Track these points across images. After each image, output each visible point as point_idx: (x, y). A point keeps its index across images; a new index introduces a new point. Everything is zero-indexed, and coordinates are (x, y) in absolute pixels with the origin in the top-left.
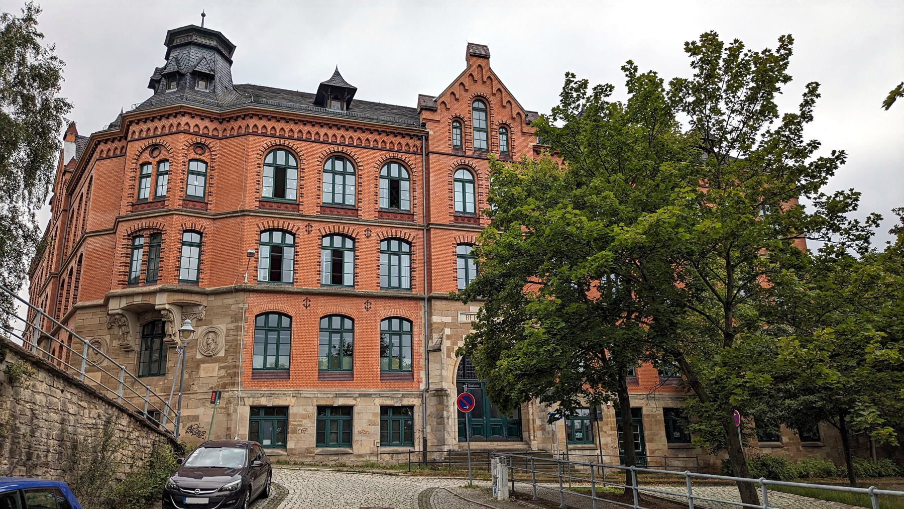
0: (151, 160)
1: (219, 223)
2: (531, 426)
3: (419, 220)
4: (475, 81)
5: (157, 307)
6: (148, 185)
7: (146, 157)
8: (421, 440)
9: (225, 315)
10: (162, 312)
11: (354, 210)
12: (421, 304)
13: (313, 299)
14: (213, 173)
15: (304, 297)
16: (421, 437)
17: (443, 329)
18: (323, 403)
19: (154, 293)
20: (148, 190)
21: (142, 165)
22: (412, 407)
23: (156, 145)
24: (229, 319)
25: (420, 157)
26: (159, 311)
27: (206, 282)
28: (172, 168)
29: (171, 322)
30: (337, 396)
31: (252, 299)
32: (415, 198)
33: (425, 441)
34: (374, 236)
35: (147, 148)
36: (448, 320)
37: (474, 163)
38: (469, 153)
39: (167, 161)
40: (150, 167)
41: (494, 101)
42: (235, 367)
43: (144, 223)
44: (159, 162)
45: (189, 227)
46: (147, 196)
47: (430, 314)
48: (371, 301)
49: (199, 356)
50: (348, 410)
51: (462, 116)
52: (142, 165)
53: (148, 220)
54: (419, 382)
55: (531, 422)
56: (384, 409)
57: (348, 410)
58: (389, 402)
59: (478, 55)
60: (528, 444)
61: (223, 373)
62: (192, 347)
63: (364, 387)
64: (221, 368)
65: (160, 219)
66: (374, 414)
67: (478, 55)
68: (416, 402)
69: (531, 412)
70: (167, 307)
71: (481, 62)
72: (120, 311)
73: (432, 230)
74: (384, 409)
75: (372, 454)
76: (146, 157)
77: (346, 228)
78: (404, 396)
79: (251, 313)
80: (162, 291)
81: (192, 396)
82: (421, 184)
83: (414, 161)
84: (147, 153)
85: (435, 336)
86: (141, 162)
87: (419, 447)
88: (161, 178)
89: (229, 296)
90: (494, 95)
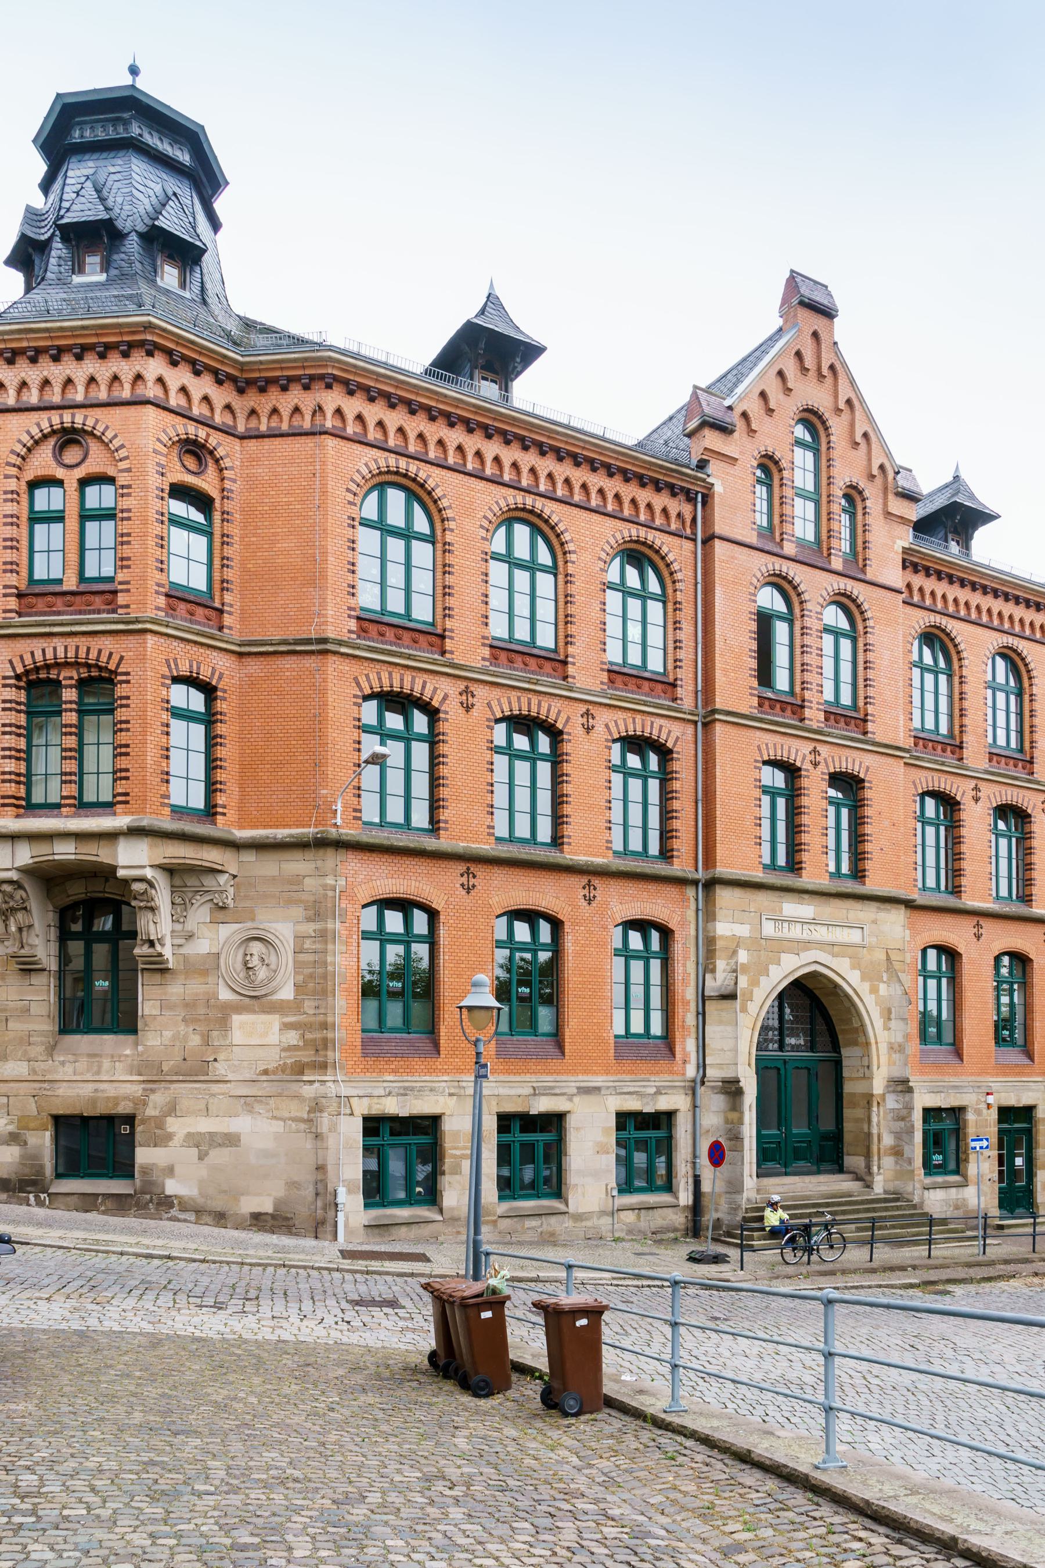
0: (60, 473)
1: (254, 667)
2: (875, 1148)
3: (686, 694)
4: (804, 370)
5: (121, 873)
6: (57, 544)
7: (44, 462)
8: (691, 1180)
9: (290, 902)
10: (137, 887)
11: (557, 662)
12: (690, 892)
13: (478, 870)
14: (228, 528)
15: (461, 867)
16: (690, 1173)
17: (735, 953)
18: (510, 1108)
19: (111, 836)
20: (57, 558)
21: (34, 485)
22: (669, 1116)
23: (73, 430)
24: (298, 912)
25: (688, 545)
26: (126, 882)
27: (232, 814)
28: (124, 503)
29: (152, 909)
30: (535, 1093)
31: (353, 865)
32: (677, 644)
33: (697, 1181)
34: (600, 728)
35: (45, 437)
36: (743, 930)
37: (798, 573)
38: (789, 549)
39: (111, 480)
40: (56, 492)
41: (837, 426)
42: (324, 1026)
43: (59, 648)
44: (84, 482)
45: (184, 670)
46: (56, 573)
48: (596, 882)
49: (225, 995)
50: (555, 1121)
51: (778, 455)
52: (34, 485)
53: (72, 642)
54: (685, 1062)
56: (623, 1119)
57: (555, 1121)
58: (633, 1105)
59: (809, 304)
60: (864, 1178)
61: (293, 1038)
62: (205, 973)
63: (586, 1072)
64: (286, 1027)
65: (107, 644)
66: (606, 1130)
67: (809, 304)
68: (675, 1101)
69: (875, 1119)
70: (149, 873)
71: (817, 322)
72: (14, 875)
73: (718, 727)
74: (623, 1119)
75: (603, 1213)
76: (44, 462)
77: (545, 706)
78: (658, 1092)
79: (352, 898)
80: (136, 832)
81: (215, 1088)
82: (691, 612)
83: (678, 552)
84: (46, 451)
85: (721, 965)
86: (29, 475)
87: (685, 1198)
88: (91, 527)
89: (298, 854)
90: (838, 411)
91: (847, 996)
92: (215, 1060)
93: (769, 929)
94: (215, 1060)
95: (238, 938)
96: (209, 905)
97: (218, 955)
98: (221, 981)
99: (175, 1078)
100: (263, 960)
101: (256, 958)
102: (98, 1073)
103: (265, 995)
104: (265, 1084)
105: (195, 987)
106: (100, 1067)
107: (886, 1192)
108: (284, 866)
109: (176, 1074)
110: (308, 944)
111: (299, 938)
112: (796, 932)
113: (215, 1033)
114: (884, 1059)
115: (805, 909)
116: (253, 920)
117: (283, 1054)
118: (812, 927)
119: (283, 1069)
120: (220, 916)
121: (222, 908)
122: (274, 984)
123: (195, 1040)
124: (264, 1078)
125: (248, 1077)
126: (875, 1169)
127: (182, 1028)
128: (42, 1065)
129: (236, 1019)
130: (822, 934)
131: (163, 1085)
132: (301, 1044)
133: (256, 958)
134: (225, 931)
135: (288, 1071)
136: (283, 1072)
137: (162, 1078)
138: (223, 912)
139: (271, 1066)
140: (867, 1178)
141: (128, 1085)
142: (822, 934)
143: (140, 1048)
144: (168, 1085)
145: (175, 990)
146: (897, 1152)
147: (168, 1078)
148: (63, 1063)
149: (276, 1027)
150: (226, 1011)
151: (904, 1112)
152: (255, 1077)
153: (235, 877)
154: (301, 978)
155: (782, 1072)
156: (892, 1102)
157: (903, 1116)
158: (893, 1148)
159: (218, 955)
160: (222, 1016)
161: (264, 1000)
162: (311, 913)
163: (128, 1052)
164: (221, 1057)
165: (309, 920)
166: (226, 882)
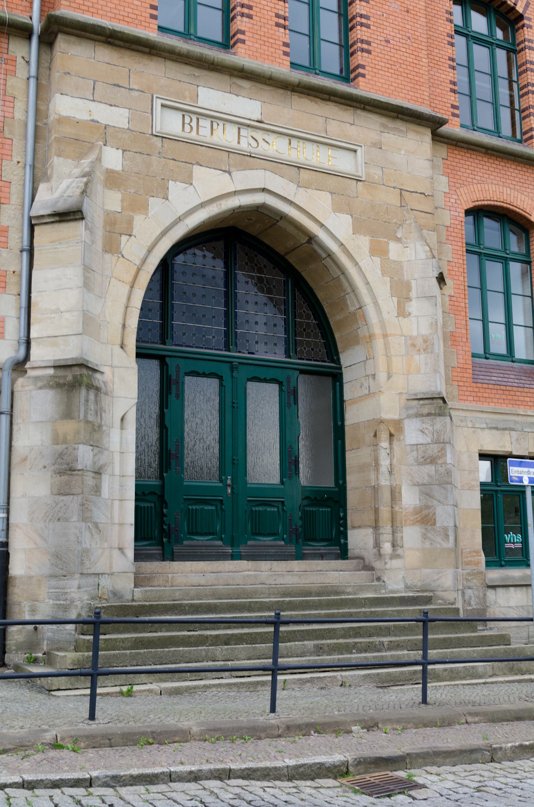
2: (385, 513)
36: (117, 117)
47: (42, 90)
55: (386, 495)
69: (384, 462)
91: (330, 255)
93: (171, 123)
107: (408, 588)
112: (226, 137)
114: (398, 364)
115: (246, 105)
118: (259, 135)
126: (387, 547)
130: (276, 147)
140: (377, 565)
142: (276, 147)
146: (425, 518)
151: (434, 450)
155: (228, 382)
156: (413, 433)
157: (431, 457)
158: (418, 511)
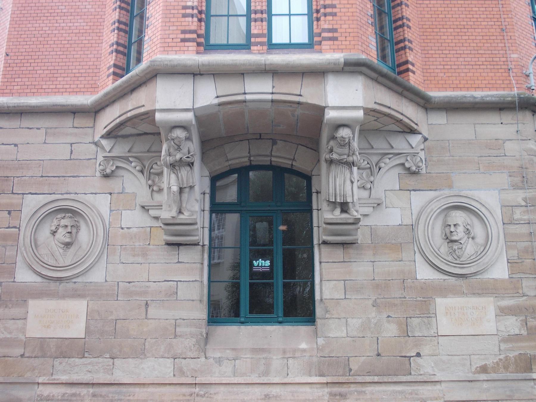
24: (503, 179)
49: (425, 273)
61: (513, 325)
62: (398, 247)
64: (503, 312)
89: (494, 118)
92: (418, 355)
94: (418, 355)
95: (436, 206)
96: (399, 170)
97: (413, 227)
98: (418, 257)
99: (368, 379)
100: (468, 232)
101: (461, 229)
102: (266, 373)
103: (475, 274)
104: (485, 385)
105: (387, 265)
106: (268, 365)
108: (479, 129)
109: (369, 374)
110: (518, 214)
111: (508, 207)
113: (415, 322)
116: (450, 187)
117: (503, 346)
119: (505, 364)
120: (411, 182)
121: (414, 173)
122: (486, 259)
123: (391, 330)
124: (483, 377)
125: (461, 375)
127: (373, 314)
128: (192, 364)
129: (441, 303)
131: (353, 388)
132: (524, 332)
133: (461, 229)
134: (418, 199)
135: (512, 368)
136: (506, 368)
137: (351, 379)
138: (414, 178)
139: (490, 362)
141: (307, 389)
143: (321, 341)
144: (359, 388)
145: (362, 268)
147: (360, 379)
148: (219, 361)
149: (491, 312)
150: (426, 296)
152: (471, 376)
153: (426, 139)
154: (515, 253)
159: (413, 227)
160: (423, 302)
161: (472, 280)
162: (517, 180)
163: (303, 346)
164: (425, 351)
165: (515, 187)
166: (418, 145)
